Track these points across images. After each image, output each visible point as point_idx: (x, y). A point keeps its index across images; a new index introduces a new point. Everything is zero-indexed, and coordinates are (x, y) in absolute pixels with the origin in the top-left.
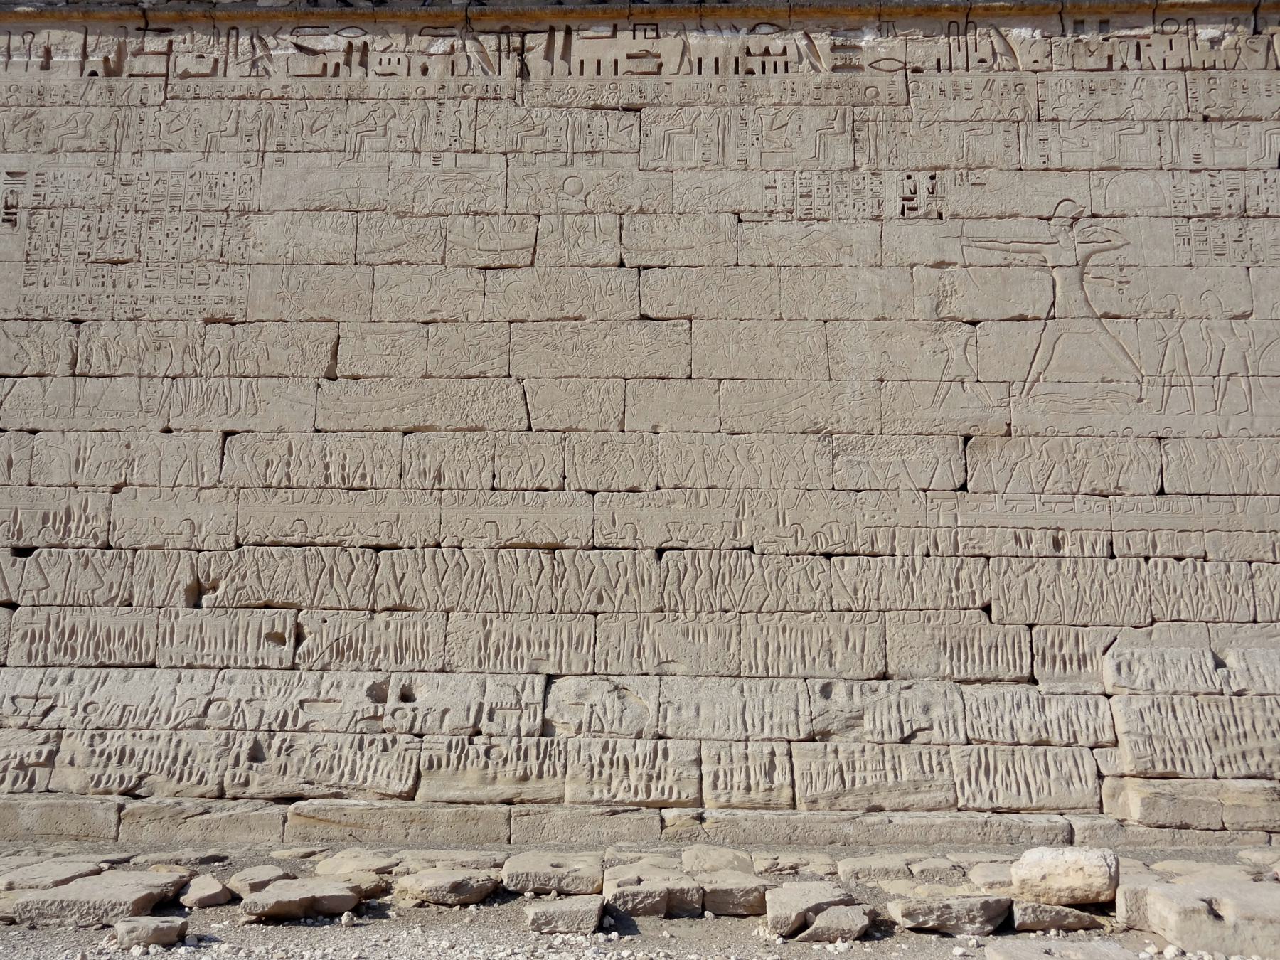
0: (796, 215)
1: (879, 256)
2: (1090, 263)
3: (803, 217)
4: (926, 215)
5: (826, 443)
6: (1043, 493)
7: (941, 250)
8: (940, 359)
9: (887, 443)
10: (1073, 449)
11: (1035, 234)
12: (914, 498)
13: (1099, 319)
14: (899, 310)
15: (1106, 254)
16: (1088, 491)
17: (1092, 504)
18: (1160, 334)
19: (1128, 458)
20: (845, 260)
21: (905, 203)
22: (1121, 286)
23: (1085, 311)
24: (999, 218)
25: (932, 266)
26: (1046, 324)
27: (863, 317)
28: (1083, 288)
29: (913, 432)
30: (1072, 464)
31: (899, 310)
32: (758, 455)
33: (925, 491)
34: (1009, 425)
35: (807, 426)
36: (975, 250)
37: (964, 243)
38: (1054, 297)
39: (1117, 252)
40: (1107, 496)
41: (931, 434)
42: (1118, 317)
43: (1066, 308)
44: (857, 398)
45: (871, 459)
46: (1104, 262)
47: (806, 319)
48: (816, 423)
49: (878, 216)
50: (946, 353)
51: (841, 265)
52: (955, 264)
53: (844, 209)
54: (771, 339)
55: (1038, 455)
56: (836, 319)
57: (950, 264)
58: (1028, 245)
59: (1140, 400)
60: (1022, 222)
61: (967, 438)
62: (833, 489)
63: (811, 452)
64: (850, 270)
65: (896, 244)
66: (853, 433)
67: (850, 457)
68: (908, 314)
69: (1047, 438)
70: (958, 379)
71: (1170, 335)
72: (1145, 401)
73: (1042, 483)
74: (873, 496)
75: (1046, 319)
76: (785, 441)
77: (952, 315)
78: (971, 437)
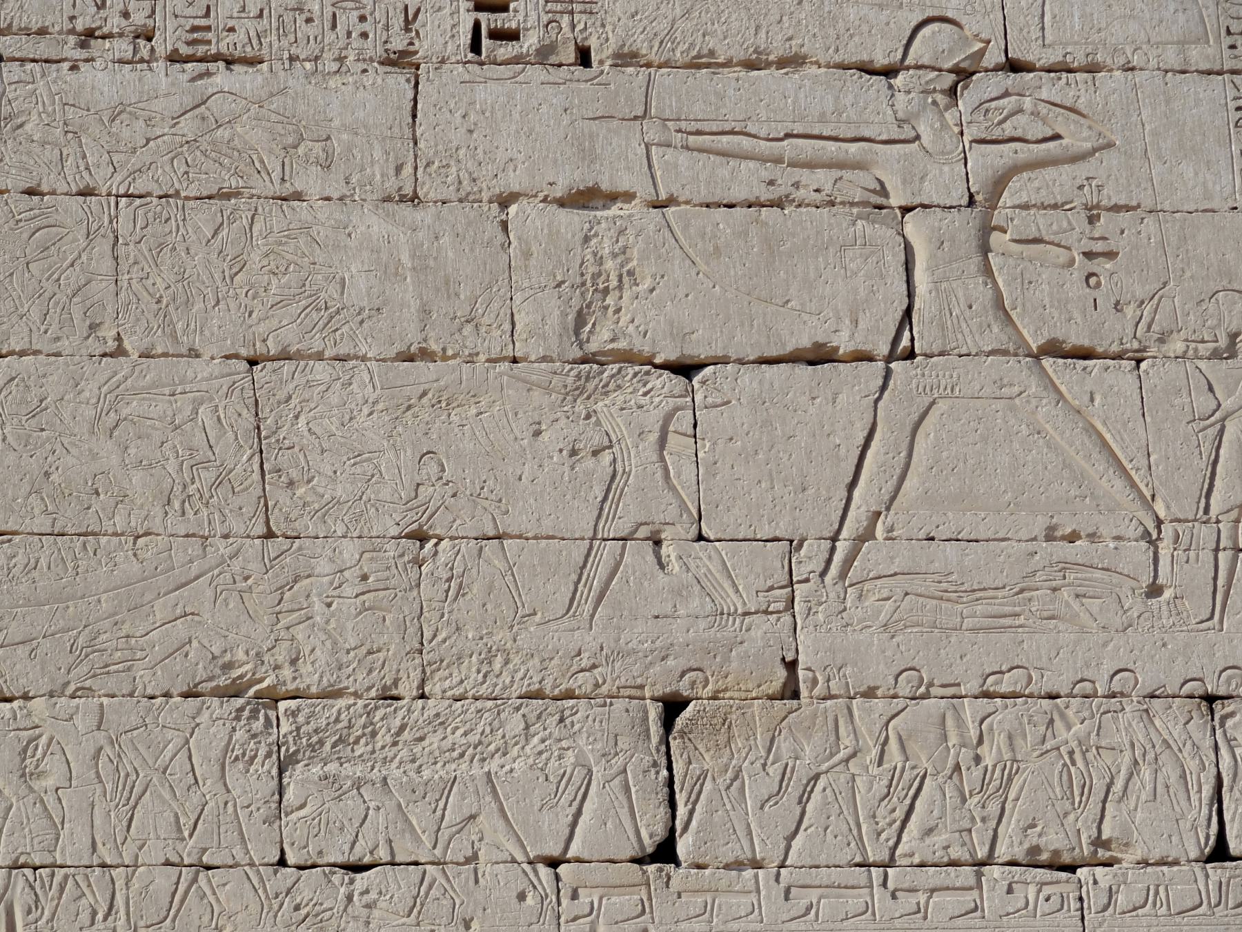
0: (162, 45)
1: (408, 170)
2: (1006, 198)
3: (185, 50)
4: (544, 55)
5: (258, 725)
6: (891, 863)
7: (588, 155)
8: (590, 474)
9: (437, 721)
10: (973, 734)
11: (852, 113)
12: (522, 884)
13: (1037, 357)
14: (468, 329)
15: (1049, 173)
16: (1019, 853)
17: (1032, 891)
18: (1204, 403)
19: (1126, 759)
20: (309, 181)
21: (483, 17)
22: (1093, 266)
23: (996, 336)
24: (750, 65)
25: (561, 203)
26: (888, 374)
27: (363, 349)
28: (987, 271)
29: (516, 691)
30: (971, 777)
31: (468, 329)
32: (54, 765)
33: (553, 863)
34: (791, 666)
35: (201, 674)
36: (683, 158)
37: (653, 135)
38: (911, 295)
39: (1082, 170)
40: (1072, 869)
41: (569, 695)
42: (1086, 354)
43: (943, 327)
44: (348, 590)
45: (394, 772)
46: (1044, 197)
47: (194, 353)
48: (228, 667)
49: (404, 54)
50: (606, 457)
51: (298, 196)
52: (629, 197)
53: (304, 29)
54: (90, 412)
55: (875, 752)
56: (285, 356)
57: (613, 197)
58: (832, 146)
59: (1155, 590)
60: (815, 79)
61: (673, 707)
62: (282, 862)
63: (215, 753)
64: (324, 211)
65: (457, 137)
66: (337, 694)
67: (332, 768)
68: (495, 342)
69: (899, 703)
70: (643, 532)
71: (1227, 404)
72: (1168, 594)
73: (890, 834)
74: (401, 882)
75: (889, 359)
76: (134, 720)
77: (622, 344)
78: (684, 704)
